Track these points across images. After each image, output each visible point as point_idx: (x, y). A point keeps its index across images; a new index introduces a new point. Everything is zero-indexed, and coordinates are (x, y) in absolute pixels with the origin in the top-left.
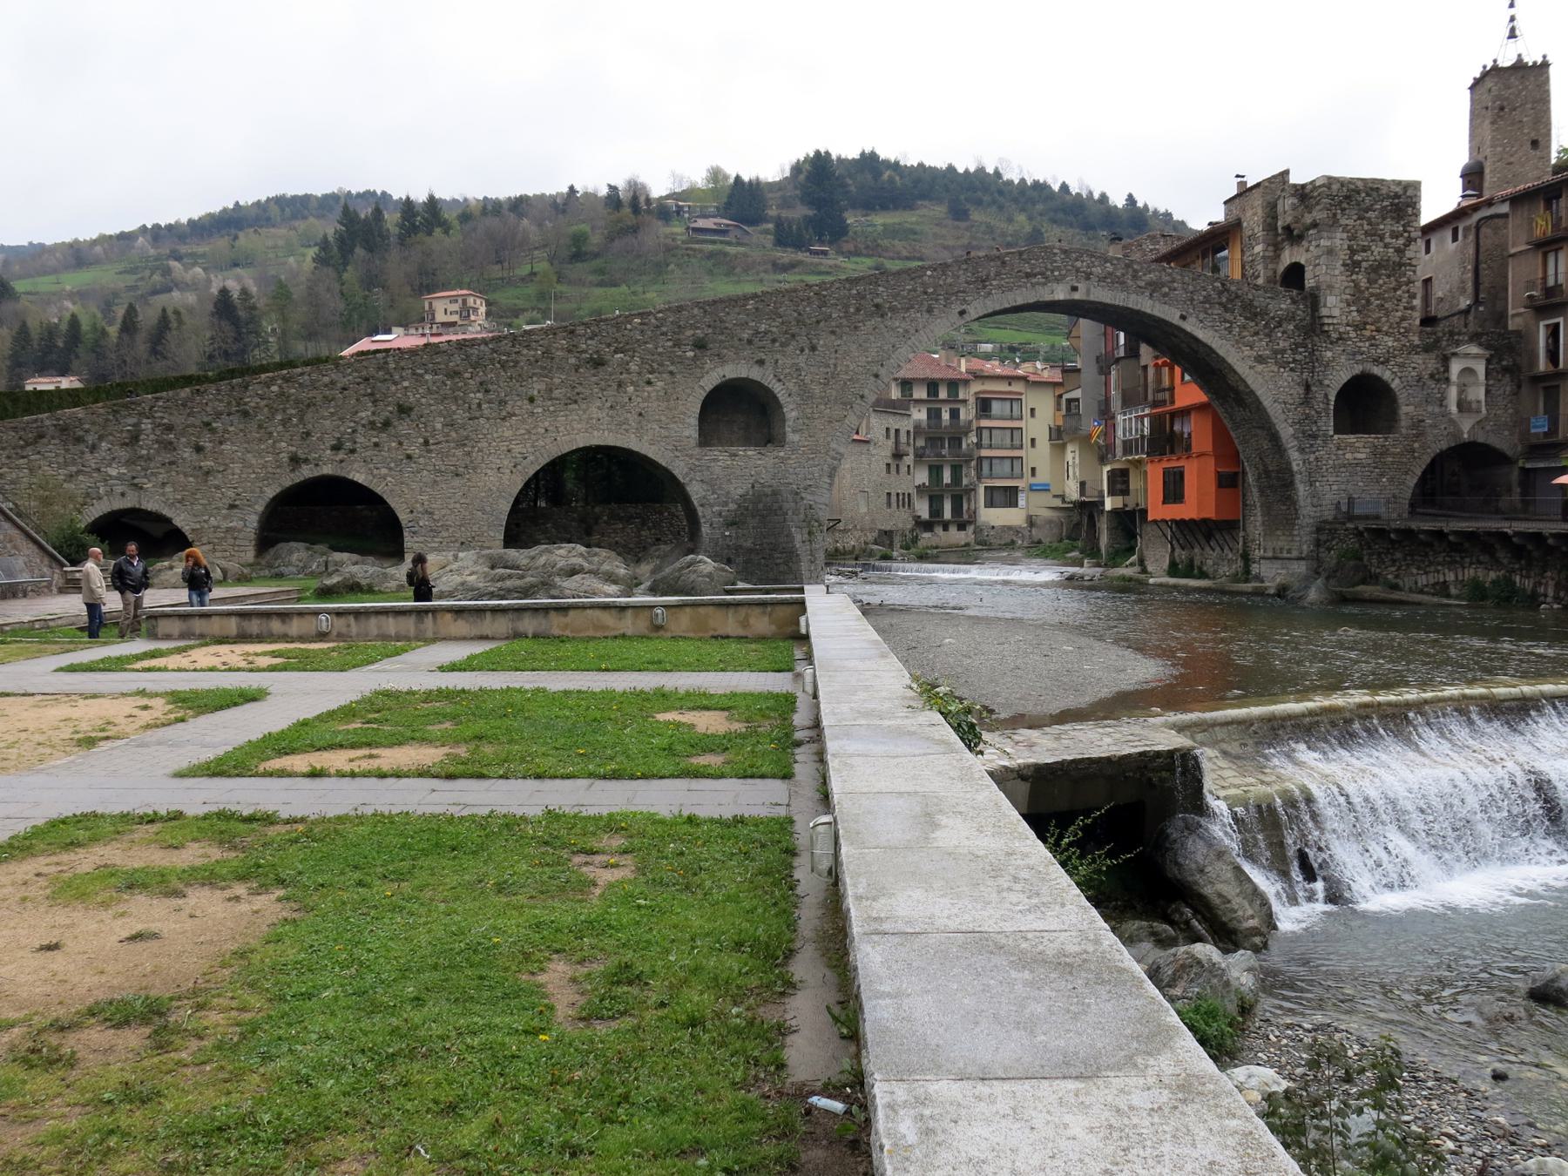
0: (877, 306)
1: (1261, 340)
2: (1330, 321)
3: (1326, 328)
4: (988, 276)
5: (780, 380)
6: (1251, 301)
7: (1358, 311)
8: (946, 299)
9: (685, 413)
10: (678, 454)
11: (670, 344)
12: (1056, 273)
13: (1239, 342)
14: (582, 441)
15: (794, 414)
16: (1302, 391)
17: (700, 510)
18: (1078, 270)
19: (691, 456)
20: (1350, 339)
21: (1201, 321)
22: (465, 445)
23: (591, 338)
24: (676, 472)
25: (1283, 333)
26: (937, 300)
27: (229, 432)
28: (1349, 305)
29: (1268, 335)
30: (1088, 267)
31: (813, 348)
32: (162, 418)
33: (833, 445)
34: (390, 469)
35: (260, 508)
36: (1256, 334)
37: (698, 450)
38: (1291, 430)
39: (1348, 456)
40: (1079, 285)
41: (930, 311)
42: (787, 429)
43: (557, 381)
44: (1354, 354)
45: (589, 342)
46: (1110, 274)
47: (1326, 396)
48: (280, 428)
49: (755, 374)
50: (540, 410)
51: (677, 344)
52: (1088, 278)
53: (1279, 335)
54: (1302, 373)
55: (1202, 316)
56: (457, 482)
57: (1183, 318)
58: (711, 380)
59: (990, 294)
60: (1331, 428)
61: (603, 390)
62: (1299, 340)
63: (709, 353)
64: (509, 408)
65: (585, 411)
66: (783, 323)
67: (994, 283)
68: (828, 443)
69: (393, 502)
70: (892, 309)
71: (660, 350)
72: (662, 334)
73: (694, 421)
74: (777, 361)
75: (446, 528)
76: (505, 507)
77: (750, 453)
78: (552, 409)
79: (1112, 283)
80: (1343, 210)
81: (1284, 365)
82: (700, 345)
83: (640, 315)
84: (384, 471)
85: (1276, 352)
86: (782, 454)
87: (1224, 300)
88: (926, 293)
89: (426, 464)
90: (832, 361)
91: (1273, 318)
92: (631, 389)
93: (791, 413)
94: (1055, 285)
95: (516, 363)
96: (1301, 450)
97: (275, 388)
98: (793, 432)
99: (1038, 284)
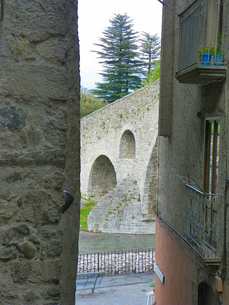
42: (136, 153)
45: (104, 116)
58: (122, 132)
72: (115, 112)
73: (118, 147)
92: (109, 134)
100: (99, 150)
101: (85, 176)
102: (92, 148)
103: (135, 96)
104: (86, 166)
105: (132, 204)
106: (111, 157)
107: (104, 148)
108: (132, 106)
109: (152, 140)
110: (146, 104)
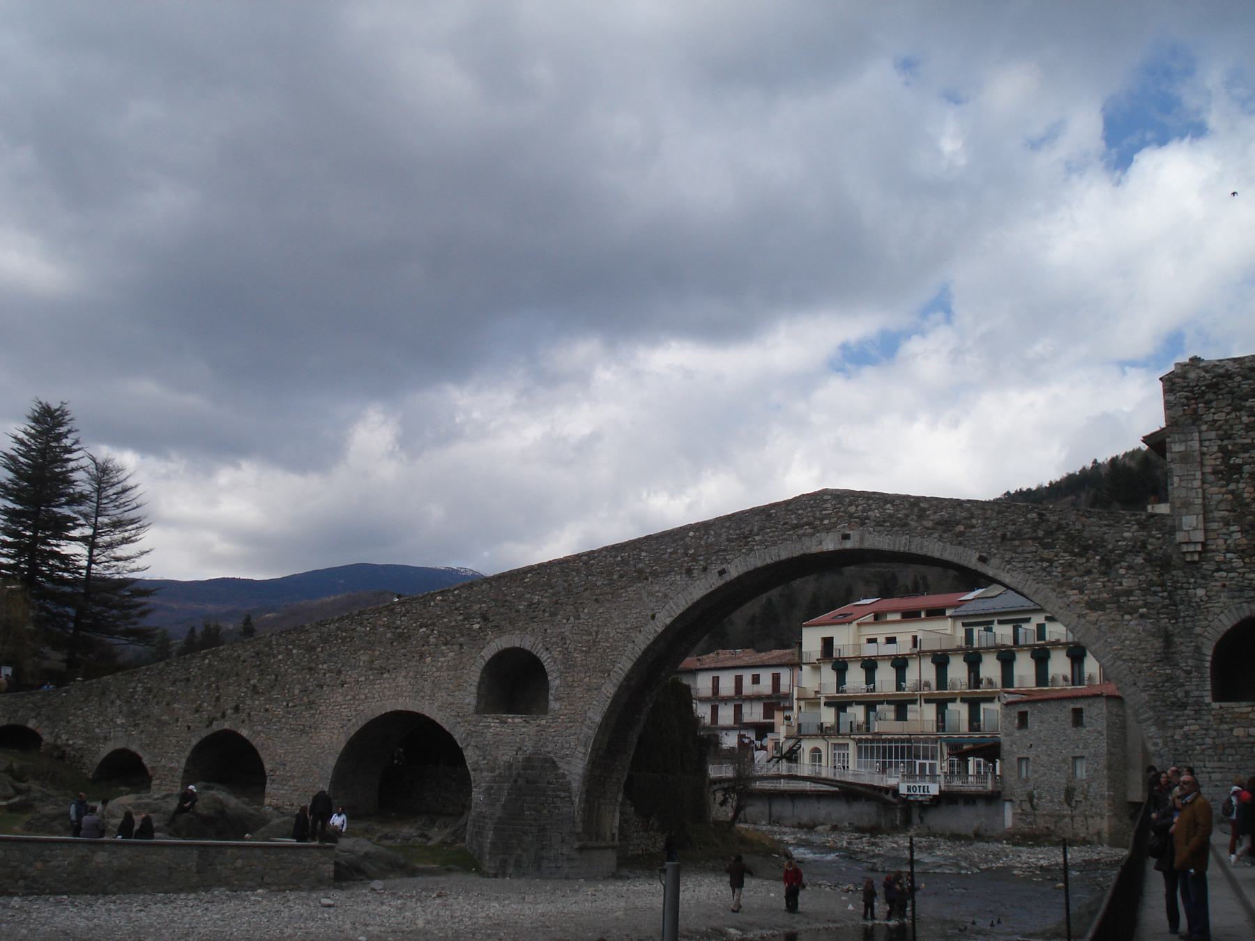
0: (640, 571)
1: (1094, 580)
2: (1191, 548)
3: (1188, 558)
4: (751, 531)
5: (547, 649)
6: (1079, 531)
7: (1242, 531)
8: (706, 560)
9: (467, 682)
10: (459, 720)
11: (461, 617)
12: (826, 522)
13: (1063, 584)
14: (390, 706)
15: (557, 682)
16: (1158, 644)
17: (472, 773)
18: (851, 516)
19: (469, 723)
20: (1233, 570)
21: (1009, 562)
22: (311, 708)
23: (405, 616)
24: (456, 737)
25: (1129, 568)
26: (697, 561)
27: (177, 694)
28: (1227, 524)
29: (1105, 574)
30: (863, 511)
31: (577, 618)
32: (148, 683)
33: (590, 714)
34: (264, 726)
35: (187, 753)
36: (1088, 572)
37: (476, 717)
38: (1145, 697)
39: (1235, 732)
40: (851, 533)
41: (689, 572)
42: (551, 697)
43: (377, 653)
44: (1242, 589)
45: (403, 618)
46: (890, 516)
47: (1198, 649)
48: (206, 692)
49: (527, 643)
50: (363, 679)
51: (468, 618)
52: (863, 524)
53: (1122, 571)
54: (1158, 620)
55: (1008, 555)
56: (304, 739)
57: (983, 559)
58: (489, 652)
59: (751, 550)
60: (1209, 693)
61: (409, 661)
62: (1155, 579)
63: (490, 625)
64: (342, 677)
65: (394, 679)
66: (554, 594)
67: (757, 538)
68: (585, 712)
69: (263, 755)
70: (655, 574)
71: (454, 623)
72: (456, 609)
73: (474, 689)
74: (546, 630)
75: (292, 777)
76: (332, 762)
77: (516, 720)
78: (372, 677)
79: (893, 526)
80: (1208, 403)
81: (1132, 611)
82: (485, 618)
83: (441, 593)
84: (260, 728)
85: (1118, 595)
86: (543, 722)
87: (1041, 533)
88: (686, 554)
89: (286, 723)
90: (595, 628)
91: (1112, 551)
92: (428, 660)
93: (554, 682)
94: (824, 535)
95: (354, 638)
96: (1161, 724)
97: (207, 661)
98: (556, 700)
99: (804, 535)
100: (381, 700)
101: (315, 767)
102: (349, 697)
103: (539, 573)
104: (317, 742)
105: (559, 810)
106: (441, 713)
107: (405, 694)
108: (529, 596)
109: (614, 666)
110: (586, 590)
